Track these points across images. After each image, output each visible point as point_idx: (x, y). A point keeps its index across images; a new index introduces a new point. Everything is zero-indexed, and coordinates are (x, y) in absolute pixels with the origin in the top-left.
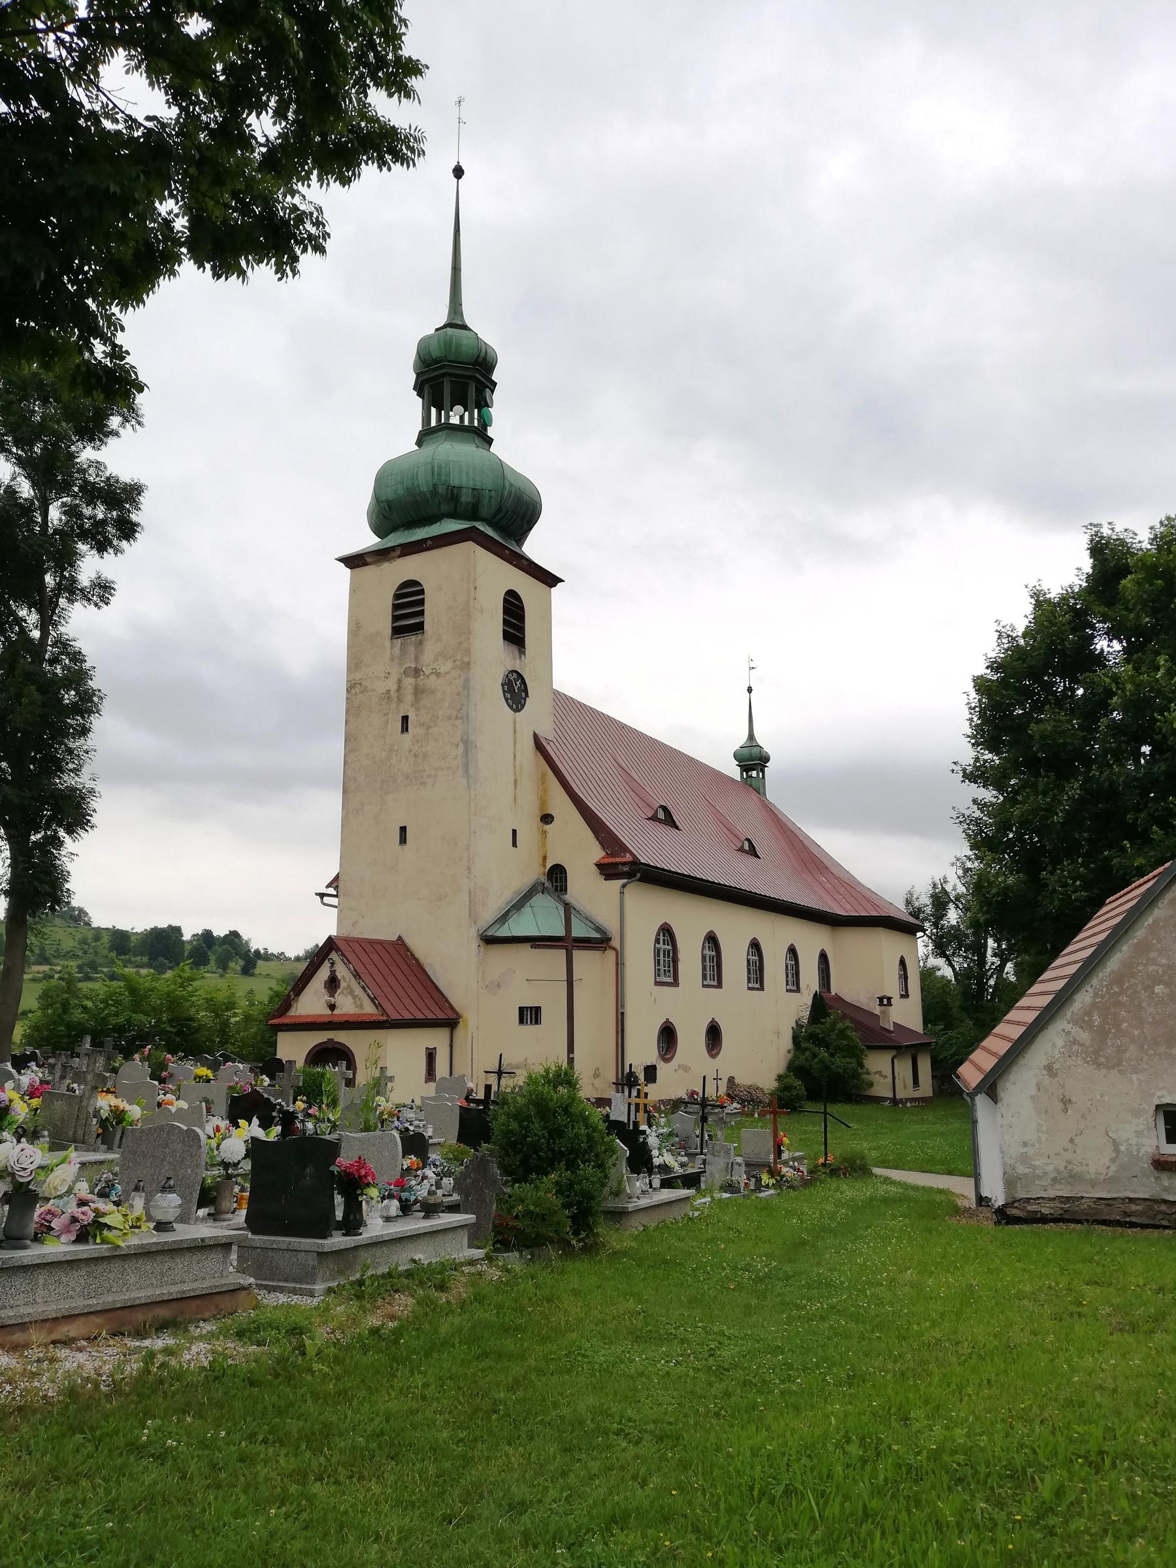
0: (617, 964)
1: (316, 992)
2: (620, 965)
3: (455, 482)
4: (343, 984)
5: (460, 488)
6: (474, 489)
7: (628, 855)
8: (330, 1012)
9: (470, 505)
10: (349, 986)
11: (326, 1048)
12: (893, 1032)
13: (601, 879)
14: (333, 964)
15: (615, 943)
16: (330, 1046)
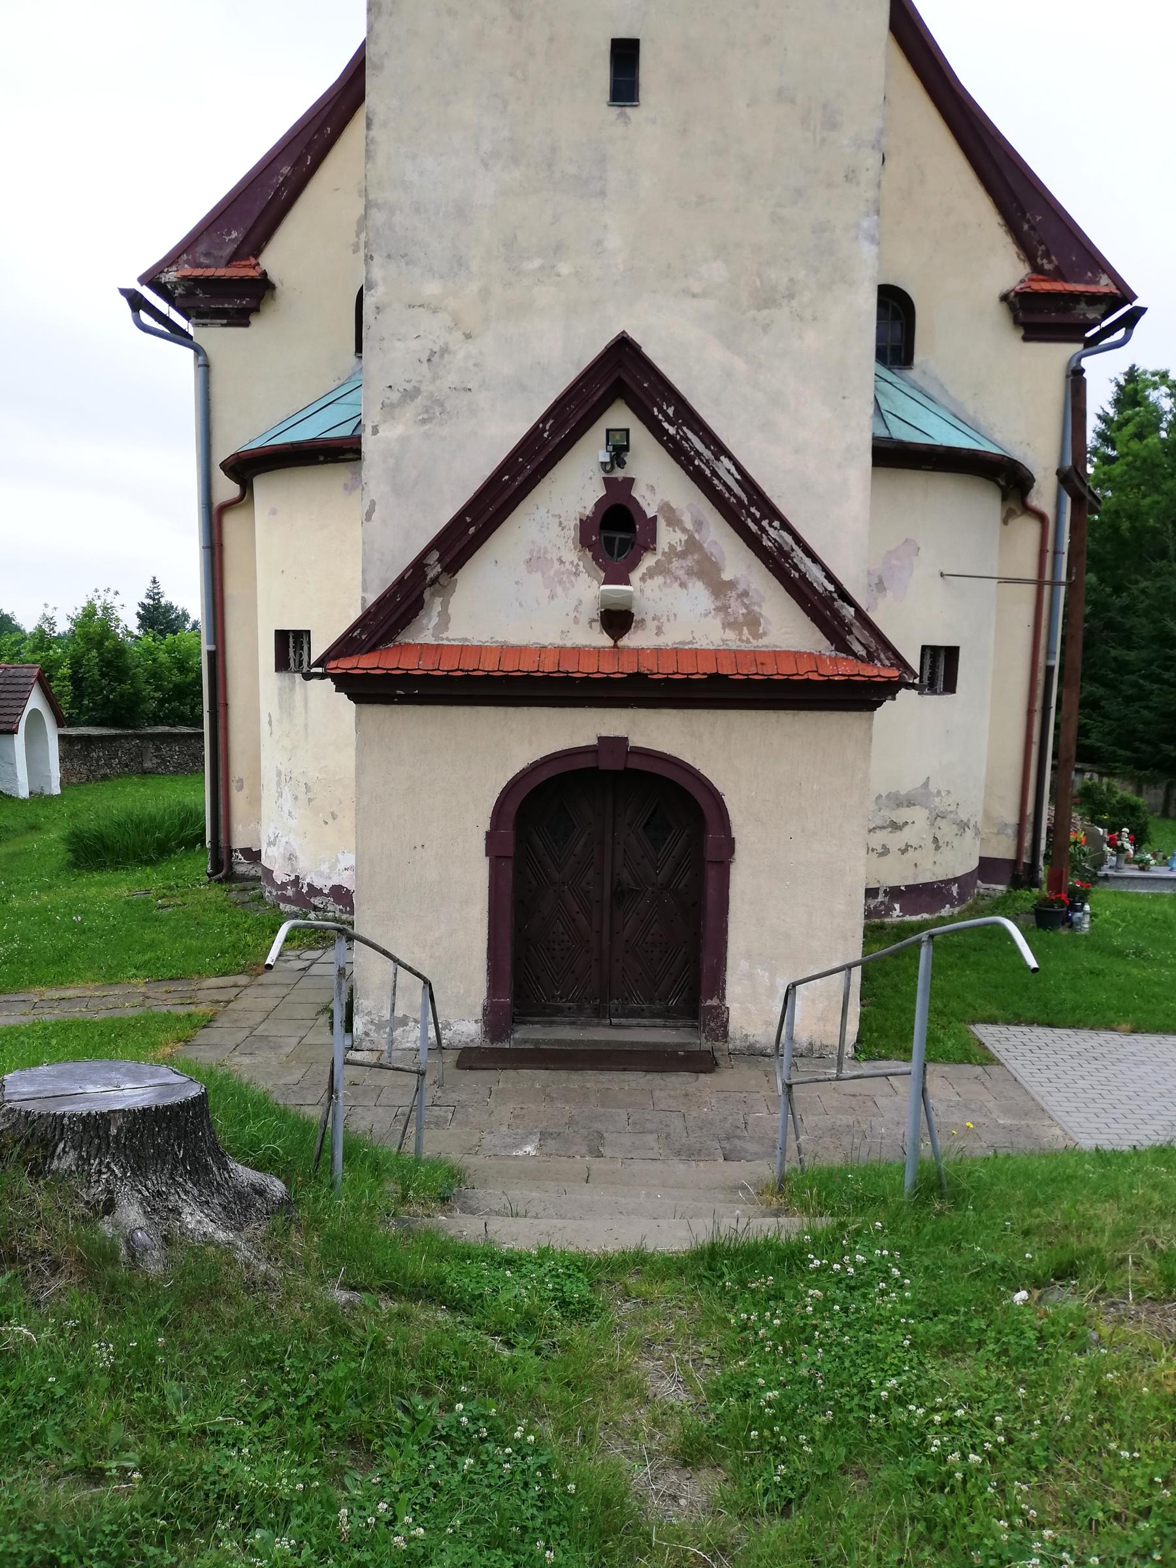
1: (535, 561)
4: (667, 537)
7: (1104, 280)
8: (605, 641)
10: (692, 545)
11: (595, 770)
13: (1012, 340)
14: (619, 451)
16: (607, 763)
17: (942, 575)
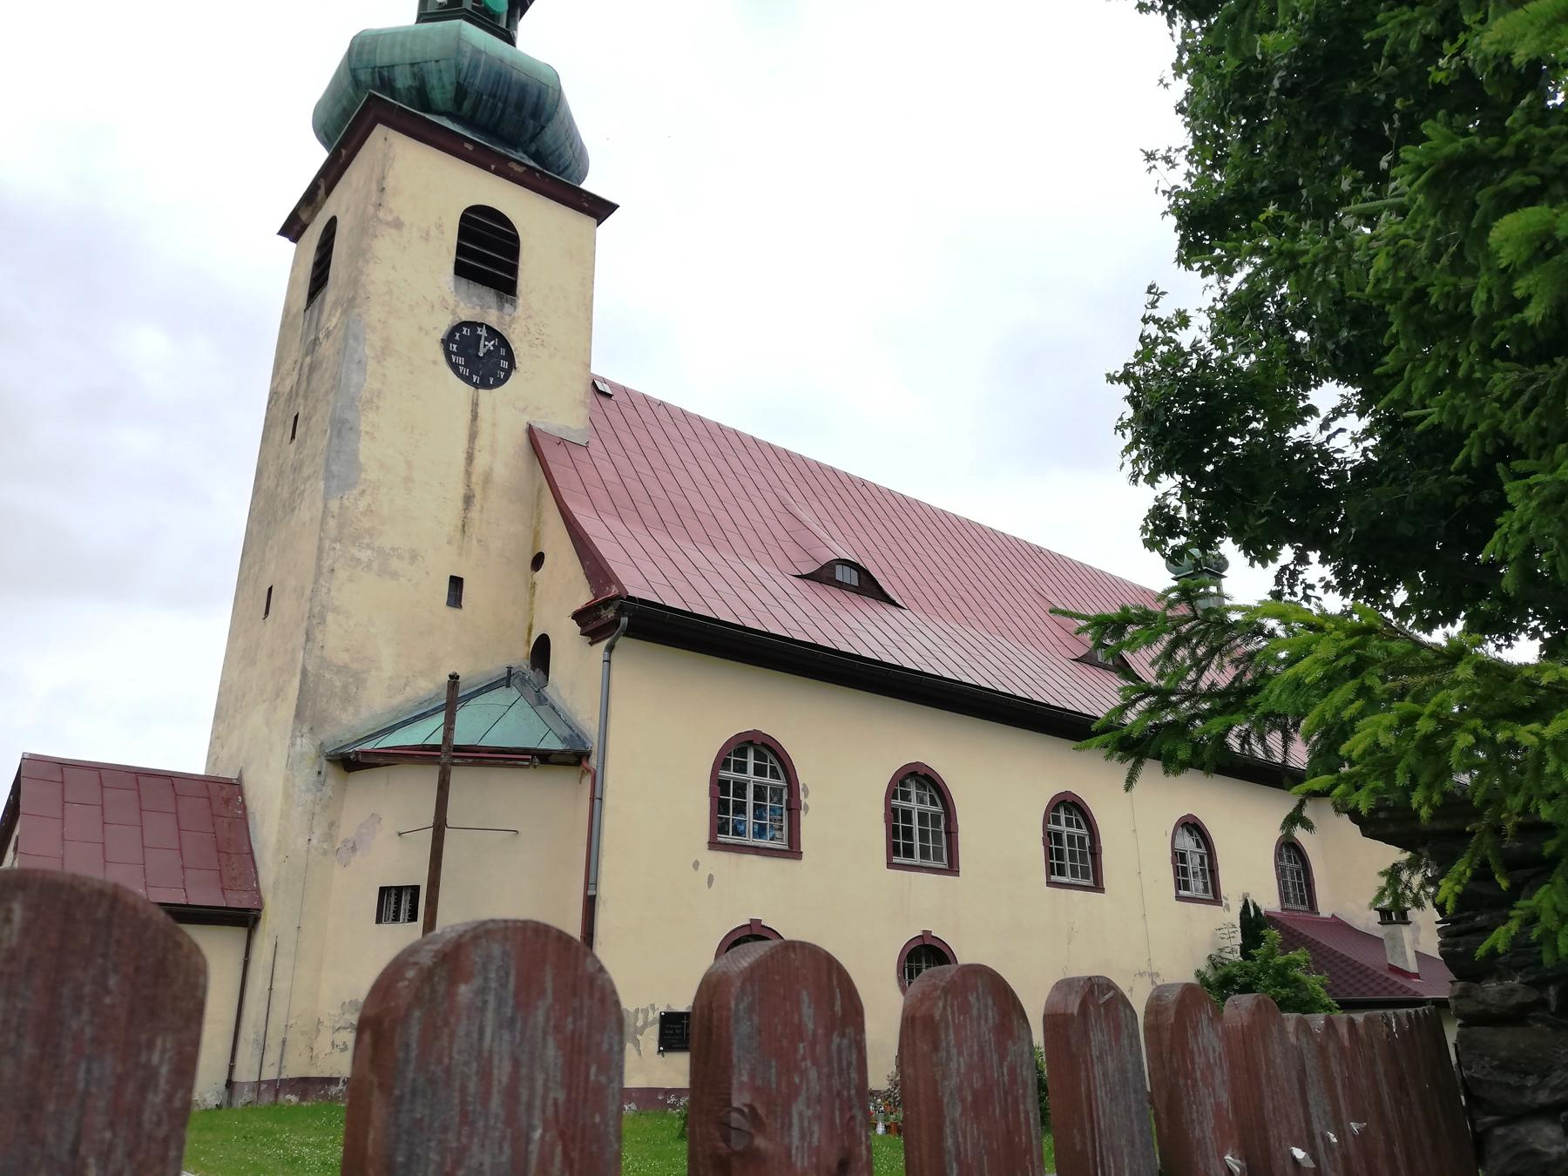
0: (592, 799)
2: (596, 799)
3: (383, 59)
5: (392, 66)
6: (412, 65)
9: (414, 92)
12: (1416, 976)
15: (594, 761)
17: (400, 834)
